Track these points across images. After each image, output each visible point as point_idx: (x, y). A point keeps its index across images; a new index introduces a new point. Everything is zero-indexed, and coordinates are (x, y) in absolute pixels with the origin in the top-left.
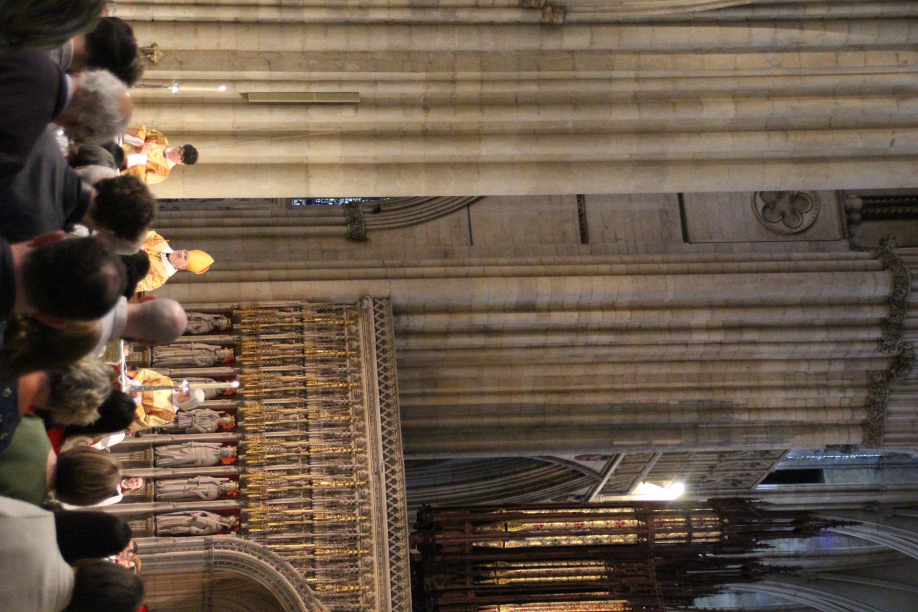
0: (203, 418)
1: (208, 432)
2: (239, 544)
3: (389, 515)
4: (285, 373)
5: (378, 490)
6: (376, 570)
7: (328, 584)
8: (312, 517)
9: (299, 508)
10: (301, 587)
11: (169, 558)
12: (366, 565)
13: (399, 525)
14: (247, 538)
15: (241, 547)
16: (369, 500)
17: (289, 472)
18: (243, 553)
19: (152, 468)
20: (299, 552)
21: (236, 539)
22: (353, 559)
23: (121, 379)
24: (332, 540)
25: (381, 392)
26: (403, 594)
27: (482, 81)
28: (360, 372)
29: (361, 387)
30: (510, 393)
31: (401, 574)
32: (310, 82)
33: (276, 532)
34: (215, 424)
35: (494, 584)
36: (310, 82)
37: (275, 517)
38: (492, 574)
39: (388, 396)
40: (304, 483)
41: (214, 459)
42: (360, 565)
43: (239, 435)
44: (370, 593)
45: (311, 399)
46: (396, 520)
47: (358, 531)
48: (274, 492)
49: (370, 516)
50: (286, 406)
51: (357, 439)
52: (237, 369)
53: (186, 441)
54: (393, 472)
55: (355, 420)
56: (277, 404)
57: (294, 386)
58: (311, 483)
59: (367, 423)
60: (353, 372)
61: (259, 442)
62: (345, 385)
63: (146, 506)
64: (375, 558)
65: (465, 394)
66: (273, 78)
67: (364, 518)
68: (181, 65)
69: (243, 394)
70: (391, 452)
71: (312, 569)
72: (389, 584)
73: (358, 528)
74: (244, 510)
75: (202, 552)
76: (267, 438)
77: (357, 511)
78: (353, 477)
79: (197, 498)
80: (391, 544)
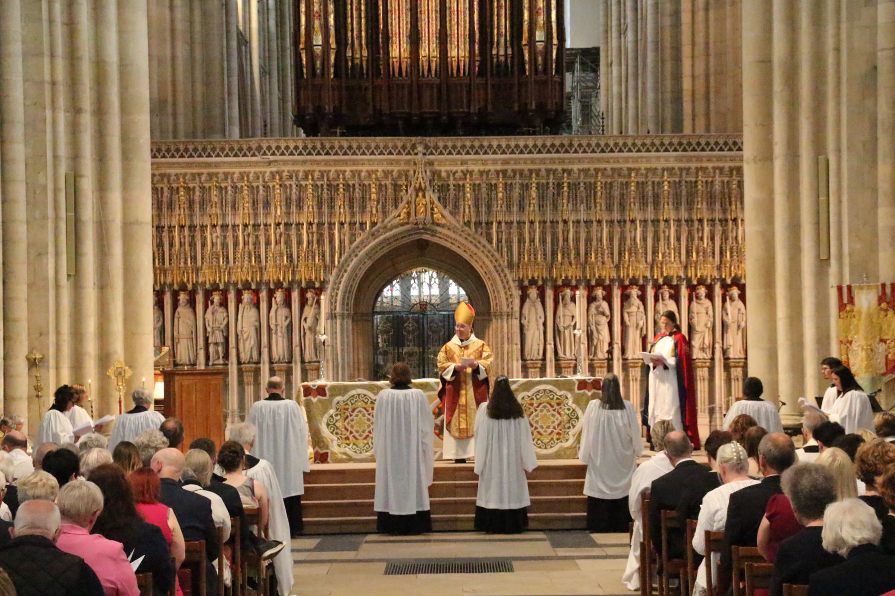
0: (215, 320)
1: (228, 316)
2: (334, 289)
3: (309, 154)
4: (171, 245)
5: (285, 163)
6: (359, 168)
7: (371, 212)
8: (310, 224)
9: (333, 234)
10: (373, 235)
11: (342, 350)
12: (354, 176)
13: (319, 146)
14: (328, 282)
15: (335, 288)
16: (294, 171)
17: (268, 243)
18: (341, 286)
19: (261, 365)
20: (342, 237)
21: (329, 291)
22: (347, 187)
23: (314, 386)
24: (331, 207)
25: (191, 156)
26: (381, 145)
27: (52, 56)
28: (169, 176)
29: (185, 175)
30: (173, 30)
31: (364, 145)
32: (57, 218)
33: (323, 256)
34: (222, 310)
35: (367, 60)
36: (57, 218)
37: (310, 257)
38: (357, 61)
39: (195, 150)
40: (278, 230)
41: (253, 311)
42: (353, 182)
43: (231, 287)
44: (379, 174)
45: (197, 221)
46: (314, 148)
47: (322, 182)
48: (287, 258)
49: (309, 171)
50: (204, 245)
51: (235, 180)
52: (167, 289)
53: (237, 335)
54: (269, 148)
55: (217, 182)
56: (202, 253)
57: (184, 237)
58: (279, 224)
59: (221, 170)
60: (169, 181)
61: (239, 270)
62: (181, 189)
63: (296, 373)
64: (348, 169)
65: (174, 74)
66: (54, 252)
67: (310, 177)
68: (43, 334)
69: (193, 284)
70: (250, 149)
71: (358, 225)
72: (373, 157)
73: (319, 183)
74: (303, 285)
75: (338, 321)
76: (234, 262)
77: (303, 183)
78: (271, 186)
79: (290, 327)
80: (336, 154)
